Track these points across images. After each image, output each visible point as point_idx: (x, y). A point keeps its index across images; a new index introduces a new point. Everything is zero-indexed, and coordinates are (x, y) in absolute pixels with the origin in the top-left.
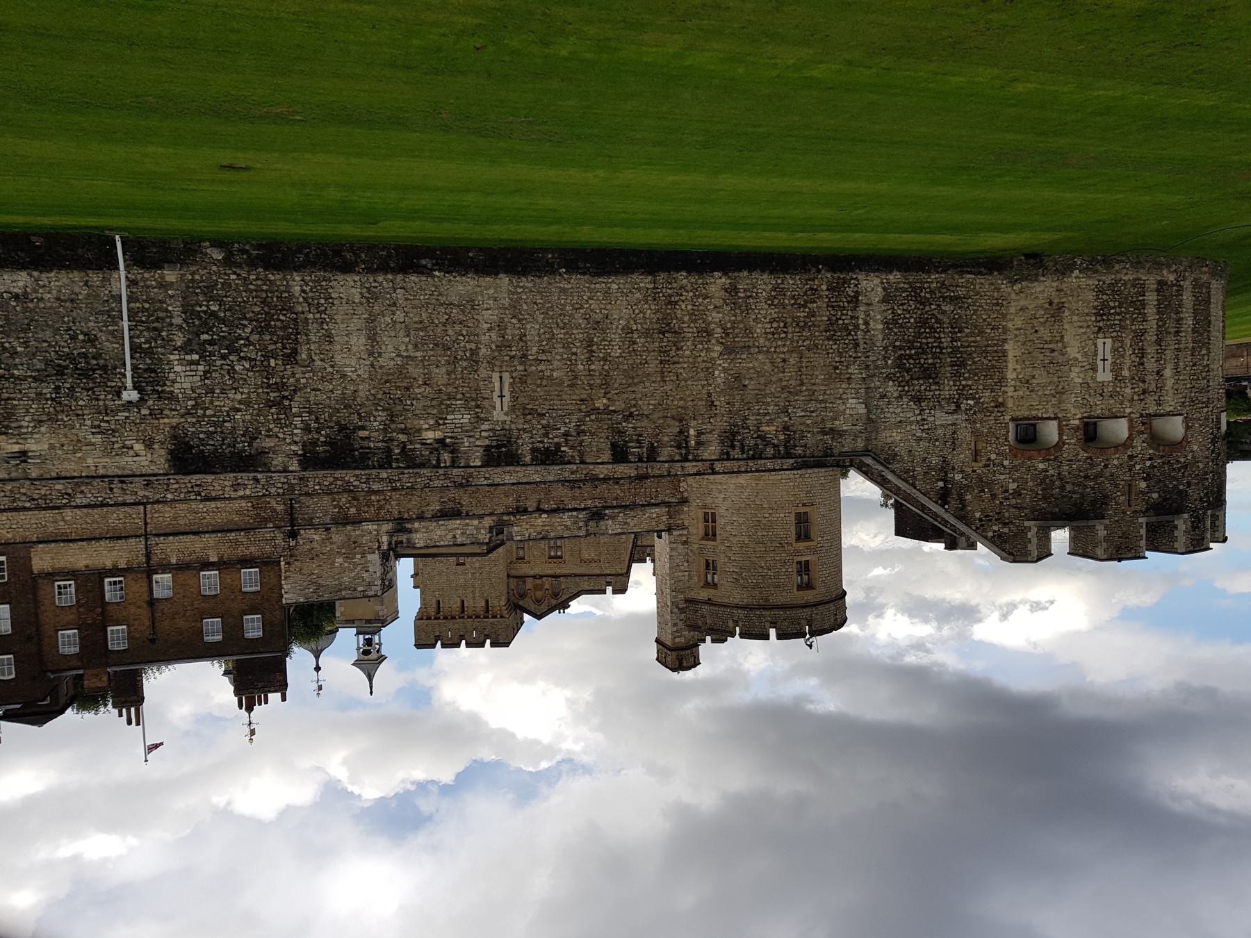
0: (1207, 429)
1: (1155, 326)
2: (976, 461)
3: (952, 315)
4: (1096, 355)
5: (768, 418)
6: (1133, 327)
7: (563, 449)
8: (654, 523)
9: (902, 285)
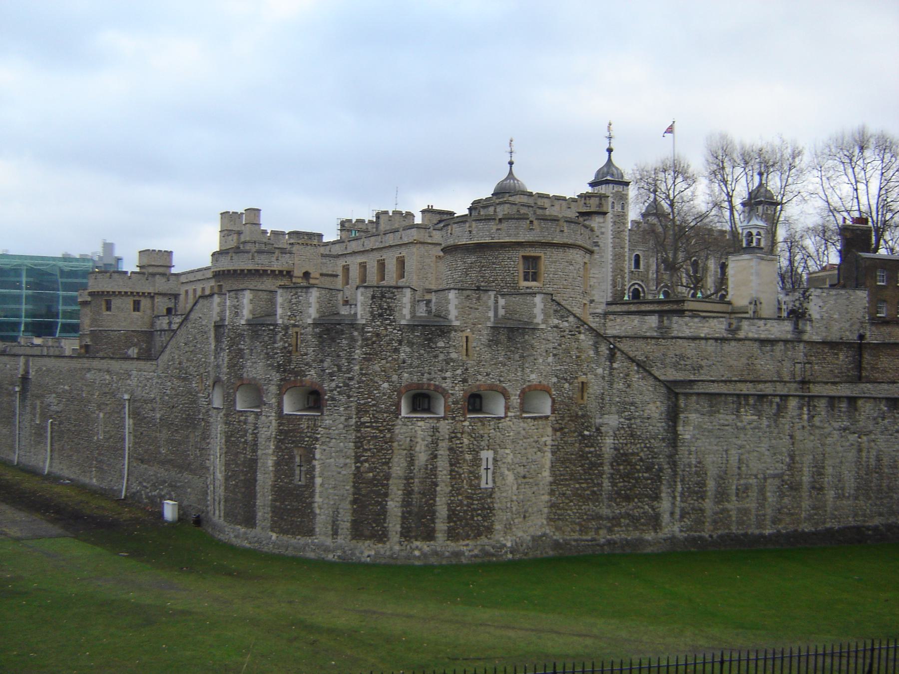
0: (362, 402)
1: (437, 499)
2: (583, 383)
3: (601, 505)
4: (494, 473)
5: (752, 426)
6: (460, 497)
7: (886, 408)
8: (618, 320)
9: (645, 528)
